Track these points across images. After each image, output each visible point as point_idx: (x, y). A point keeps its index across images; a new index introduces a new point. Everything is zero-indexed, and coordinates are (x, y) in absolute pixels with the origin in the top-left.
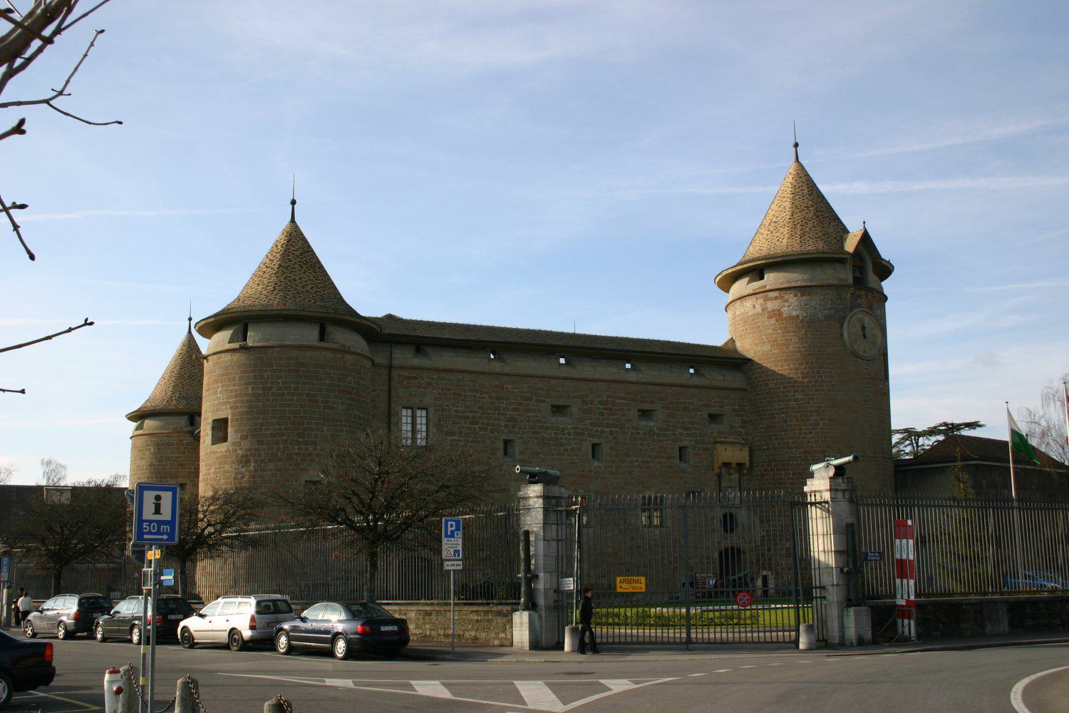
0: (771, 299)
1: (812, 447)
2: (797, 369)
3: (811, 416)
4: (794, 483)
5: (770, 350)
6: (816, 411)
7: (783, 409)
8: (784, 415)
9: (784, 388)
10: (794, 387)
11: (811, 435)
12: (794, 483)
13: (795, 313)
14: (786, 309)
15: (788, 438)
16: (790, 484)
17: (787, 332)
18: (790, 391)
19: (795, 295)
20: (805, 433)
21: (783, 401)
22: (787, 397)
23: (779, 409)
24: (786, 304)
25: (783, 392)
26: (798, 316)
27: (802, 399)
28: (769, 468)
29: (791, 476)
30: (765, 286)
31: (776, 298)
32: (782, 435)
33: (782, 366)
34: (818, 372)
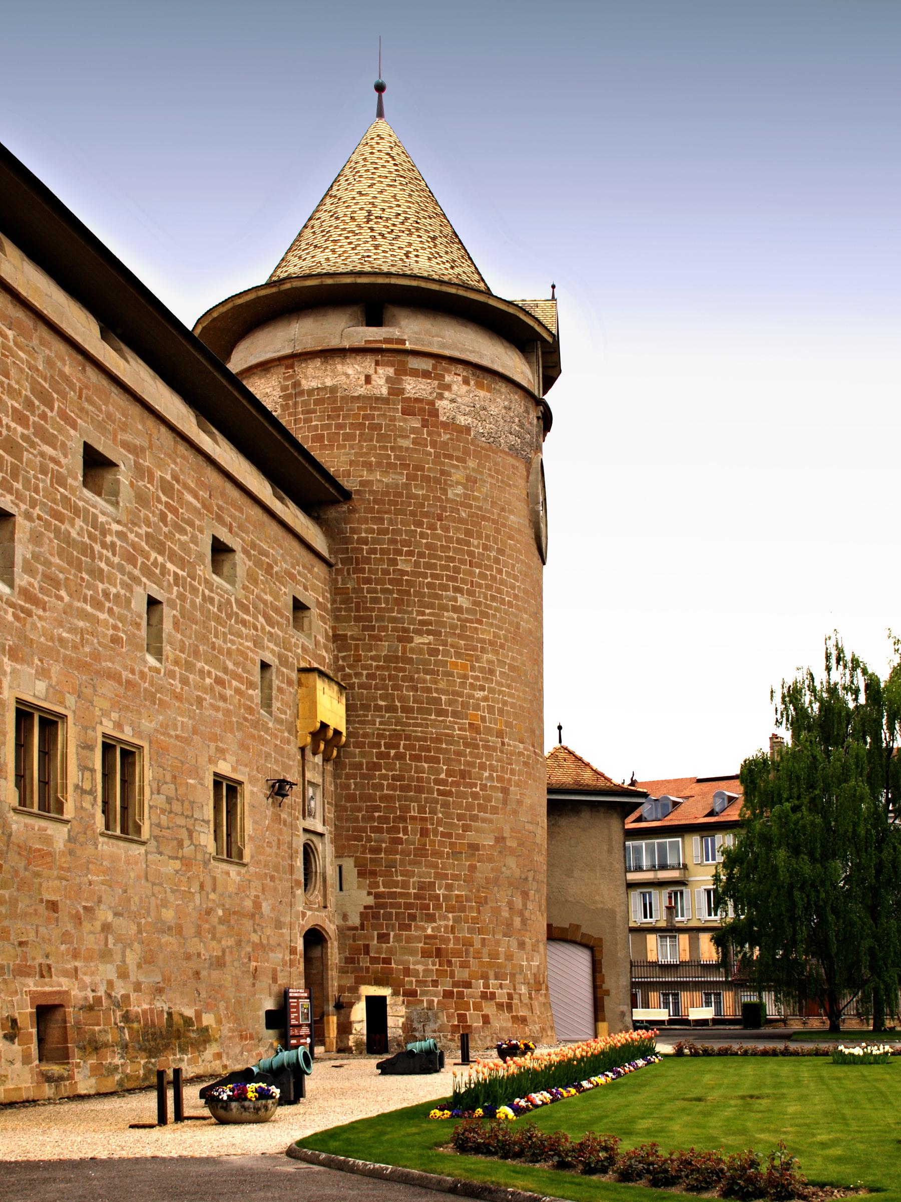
0: (415, 373)
1: (483, 719)
3: (483, 650)
4: (449, 794)
5: (407, 486)
7: (429, 623)
8: (431, 637)
9: (434, 576)
10: (454, 579)
11: (482, 693)
12: (449, 794)
16: (440, 793)
17: (446, 456)
18: (445, 588)
19: (466, 382)
21: (431, 605)
22: (439, 597)
23: (422, 623)
24: (447, 394)
25: (430, 586)
26: (468, 429)
28: (393, 752)
29: (443, 776)
30: (403, 342)
32: (425, 681)
33: (432, 527)
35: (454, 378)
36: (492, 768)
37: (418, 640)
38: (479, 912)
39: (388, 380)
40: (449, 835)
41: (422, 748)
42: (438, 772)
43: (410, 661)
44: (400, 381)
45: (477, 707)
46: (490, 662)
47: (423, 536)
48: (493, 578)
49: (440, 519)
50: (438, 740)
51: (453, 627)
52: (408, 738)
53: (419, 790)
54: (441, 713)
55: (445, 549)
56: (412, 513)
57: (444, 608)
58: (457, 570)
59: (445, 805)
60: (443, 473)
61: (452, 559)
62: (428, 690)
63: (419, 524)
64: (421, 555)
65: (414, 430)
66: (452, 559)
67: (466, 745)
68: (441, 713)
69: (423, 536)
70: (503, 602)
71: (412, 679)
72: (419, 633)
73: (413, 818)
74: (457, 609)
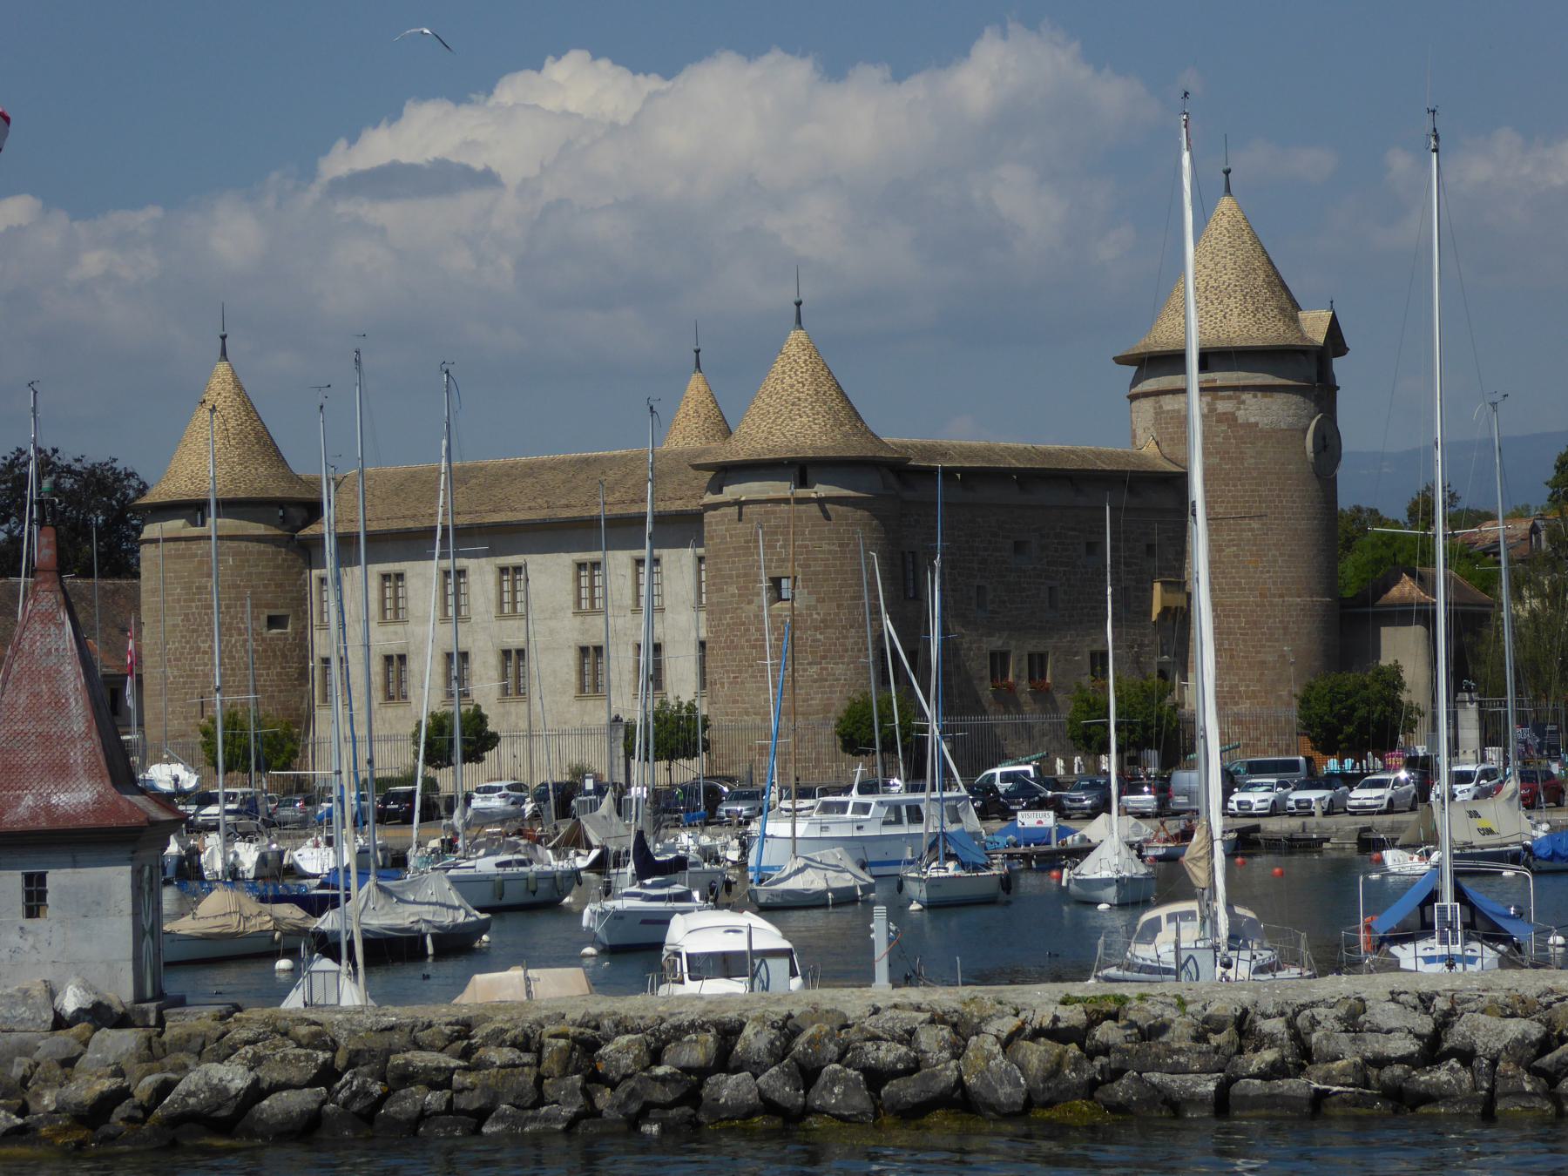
0: (1223, 398)
1: (1269, 589)
2: (1252, 491)
3: (1269, 550)
6: (1274, 545)
13: (1252, 420)
14: (1242, 412)
15: (1239, 577)
16: (1241, 634)
19: (1255, 396)
20: (1262, 572)
22: (1241, 525)
23: (1230, 540)
24: (1242, 407)
27: (1259, 529)
30: (1215, 381)
31: (1230, 398)
33: (1235, 486)
34: (1279, 496)
35: (1246, 396)
36: (1275, 617)
37: (1228, 550)
38: (1266, 698)
39: (1208, 404)
40: (1247, 657)
41: (1230, 611)
42: (1240, 623)
43: (1223, 563)
44: (1215, 404)
45: (1265, 583)
46: (1274, 556)
47: (1229, 491)
48: (1276, 507)
49: (1240, 479)
50: (1239, 605)
51: (1249, 540)
52: (1222, 605)
53: (1229, 634)
54: (1243, 589)
55: (1242, 497)
56: (1223, 479)
57: (1242, 530)
58: (1251, 507)
59: (1244, 640)
60: (1241, 453)
61: (1248, 502)
62: (1234, 578)
63: (1228, 485)
64: (1229, 502)
65: (1223, 431)
66: (1248, 502)
67: (1257, 606)
68: (1243, 589)
69: (1229, 491)
70: (1283, 519)
71: (1224, 573)
72: (1228, 546)
73: (1225, 649)
74: (1252, 530)
